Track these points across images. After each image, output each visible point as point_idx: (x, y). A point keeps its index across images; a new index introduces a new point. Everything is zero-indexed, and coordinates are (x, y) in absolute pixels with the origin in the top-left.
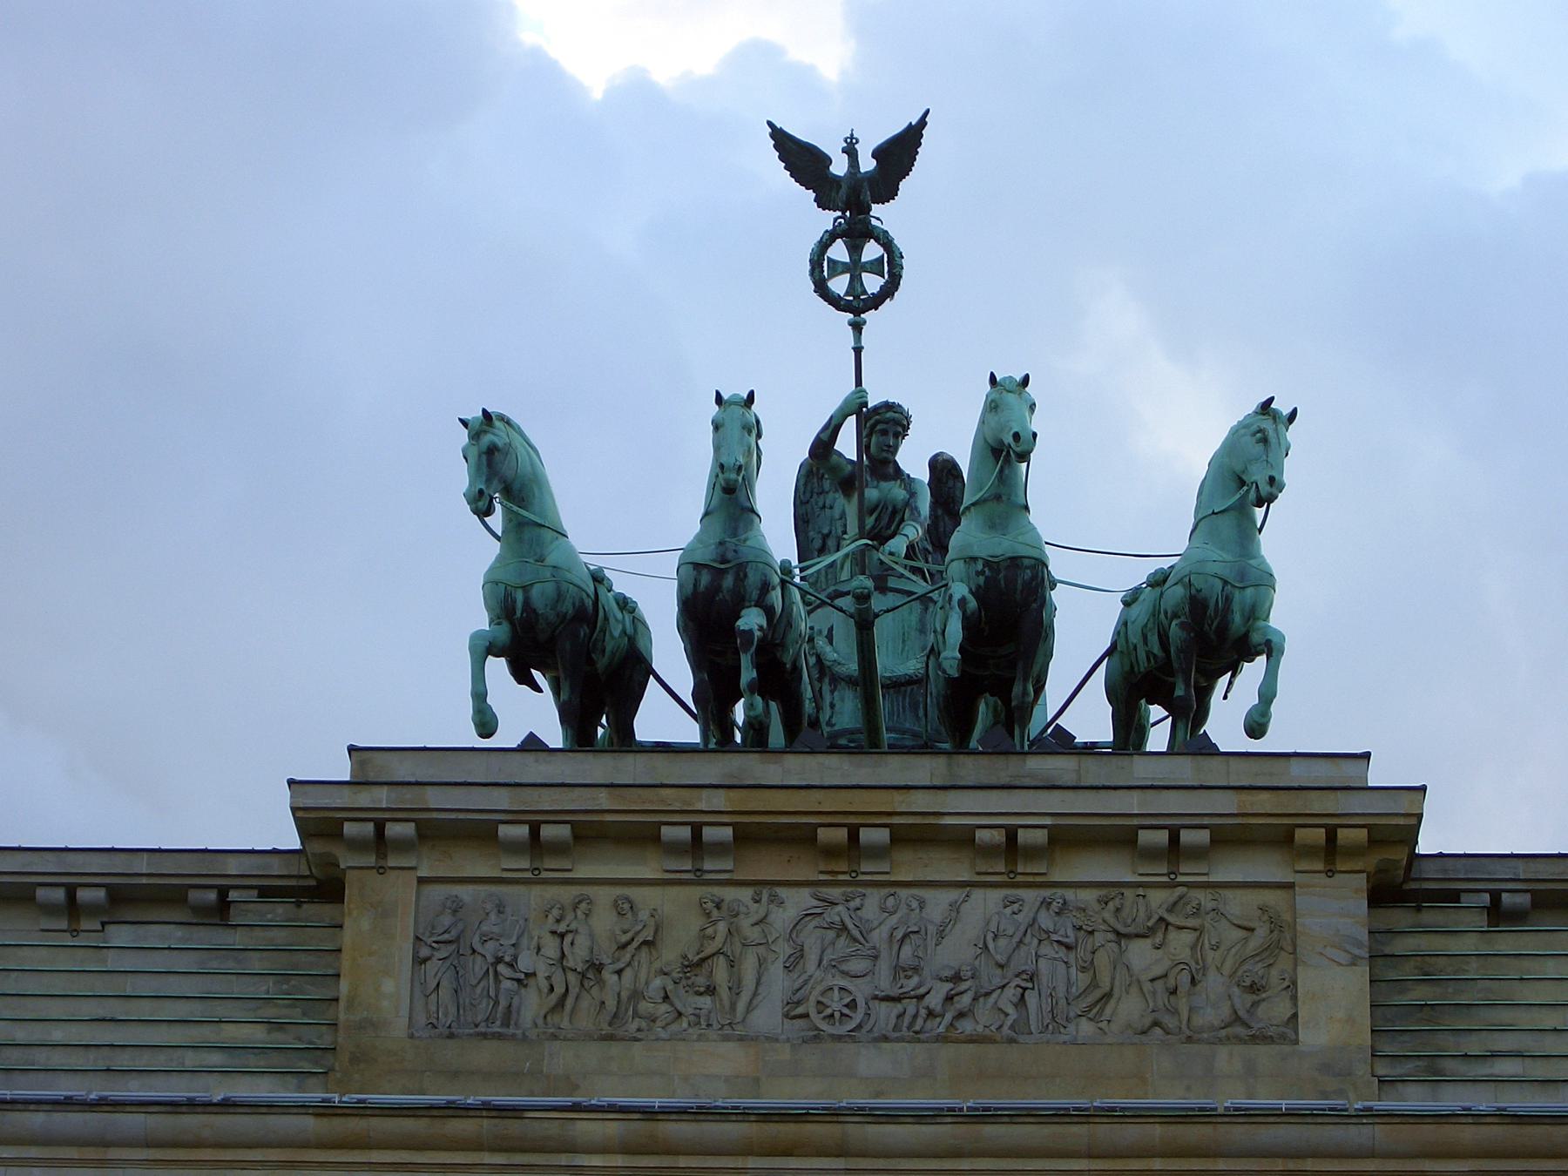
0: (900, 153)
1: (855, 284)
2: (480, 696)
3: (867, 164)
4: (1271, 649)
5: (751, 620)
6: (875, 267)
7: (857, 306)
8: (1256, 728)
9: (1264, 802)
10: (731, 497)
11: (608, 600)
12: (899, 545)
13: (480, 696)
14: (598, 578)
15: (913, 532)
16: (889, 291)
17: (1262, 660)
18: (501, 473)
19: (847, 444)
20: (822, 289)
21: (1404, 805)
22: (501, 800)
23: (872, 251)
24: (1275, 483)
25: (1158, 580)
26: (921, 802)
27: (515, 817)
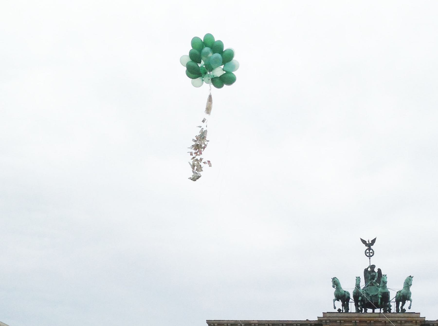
0: (374, 241)
1: (370, 255)
2: (334, 305)
3: (370, 242)
4: (411, 301)
5: (360, 298)
6: (371, 253)
7: (370, 256)
8: (409, 308)
9: (410, 319)
10: (358, 286)
11: (346, 294)
12: (374, 281)
13: (334, 305)
14: (345, 291)
15: (376, 279)
16: (373, 255)
17: (409, 301)
18: (336, 283)
19: (369, 269)
20: (366, 255)
21: (423, 319)
22: (337, 319)
23: (371, 251)
24: (411, 285)
25: (400, 292)
26: (377, 319)
27: (338, 320)
